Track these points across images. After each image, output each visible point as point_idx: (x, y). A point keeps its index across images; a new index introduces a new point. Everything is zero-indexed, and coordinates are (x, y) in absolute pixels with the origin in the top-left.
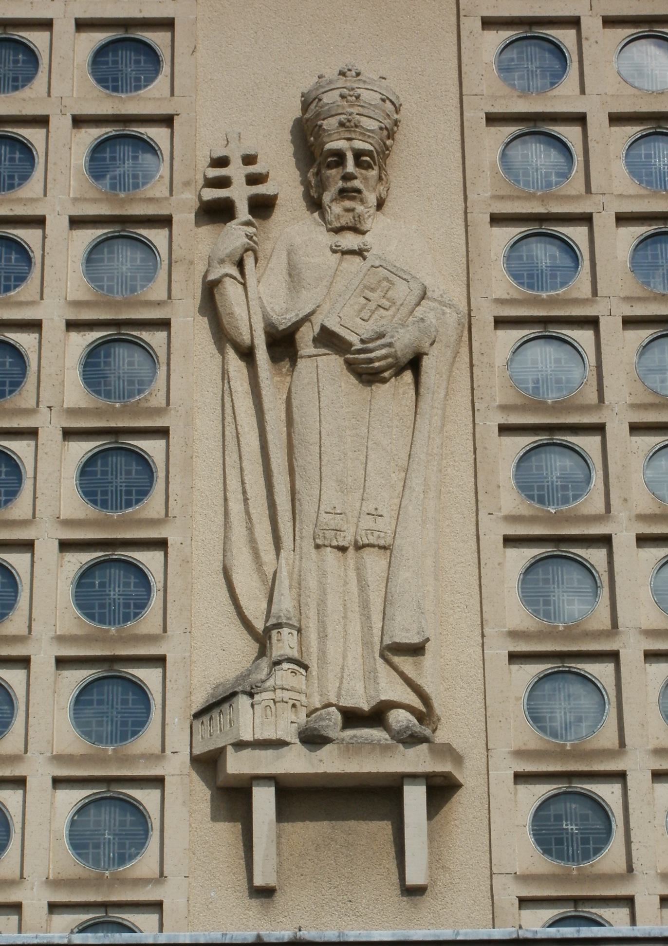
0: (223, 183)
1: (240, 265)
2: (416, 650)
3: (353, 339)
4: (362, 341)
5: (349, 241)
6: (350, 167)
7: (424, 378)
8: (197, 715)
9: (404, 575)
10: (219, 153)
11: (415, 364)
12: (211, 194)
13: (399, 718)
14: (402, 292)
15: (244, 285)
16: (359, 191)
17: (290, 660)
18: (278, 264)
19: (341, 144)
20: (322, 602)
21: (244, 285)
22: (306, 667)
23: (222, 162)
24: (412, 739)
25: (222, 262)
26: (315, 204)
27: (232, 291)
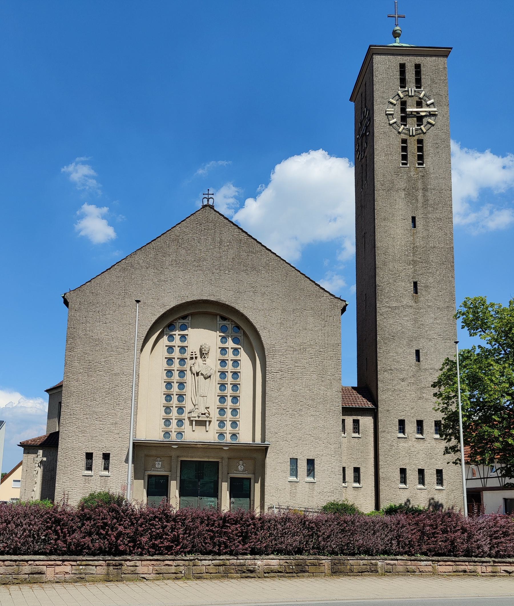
0: (192, 355)
1: (194, 365)
2: (208, 408)
6: (205, 355)
8: (188, 413)
9: (208, 400)
11: (210, 377)
13: (207, 414)
14: (209, 369)
18: (197, 364)
23: (192, 352)
24: (207, 417)
26: (201, 357)
27: (193, 368)
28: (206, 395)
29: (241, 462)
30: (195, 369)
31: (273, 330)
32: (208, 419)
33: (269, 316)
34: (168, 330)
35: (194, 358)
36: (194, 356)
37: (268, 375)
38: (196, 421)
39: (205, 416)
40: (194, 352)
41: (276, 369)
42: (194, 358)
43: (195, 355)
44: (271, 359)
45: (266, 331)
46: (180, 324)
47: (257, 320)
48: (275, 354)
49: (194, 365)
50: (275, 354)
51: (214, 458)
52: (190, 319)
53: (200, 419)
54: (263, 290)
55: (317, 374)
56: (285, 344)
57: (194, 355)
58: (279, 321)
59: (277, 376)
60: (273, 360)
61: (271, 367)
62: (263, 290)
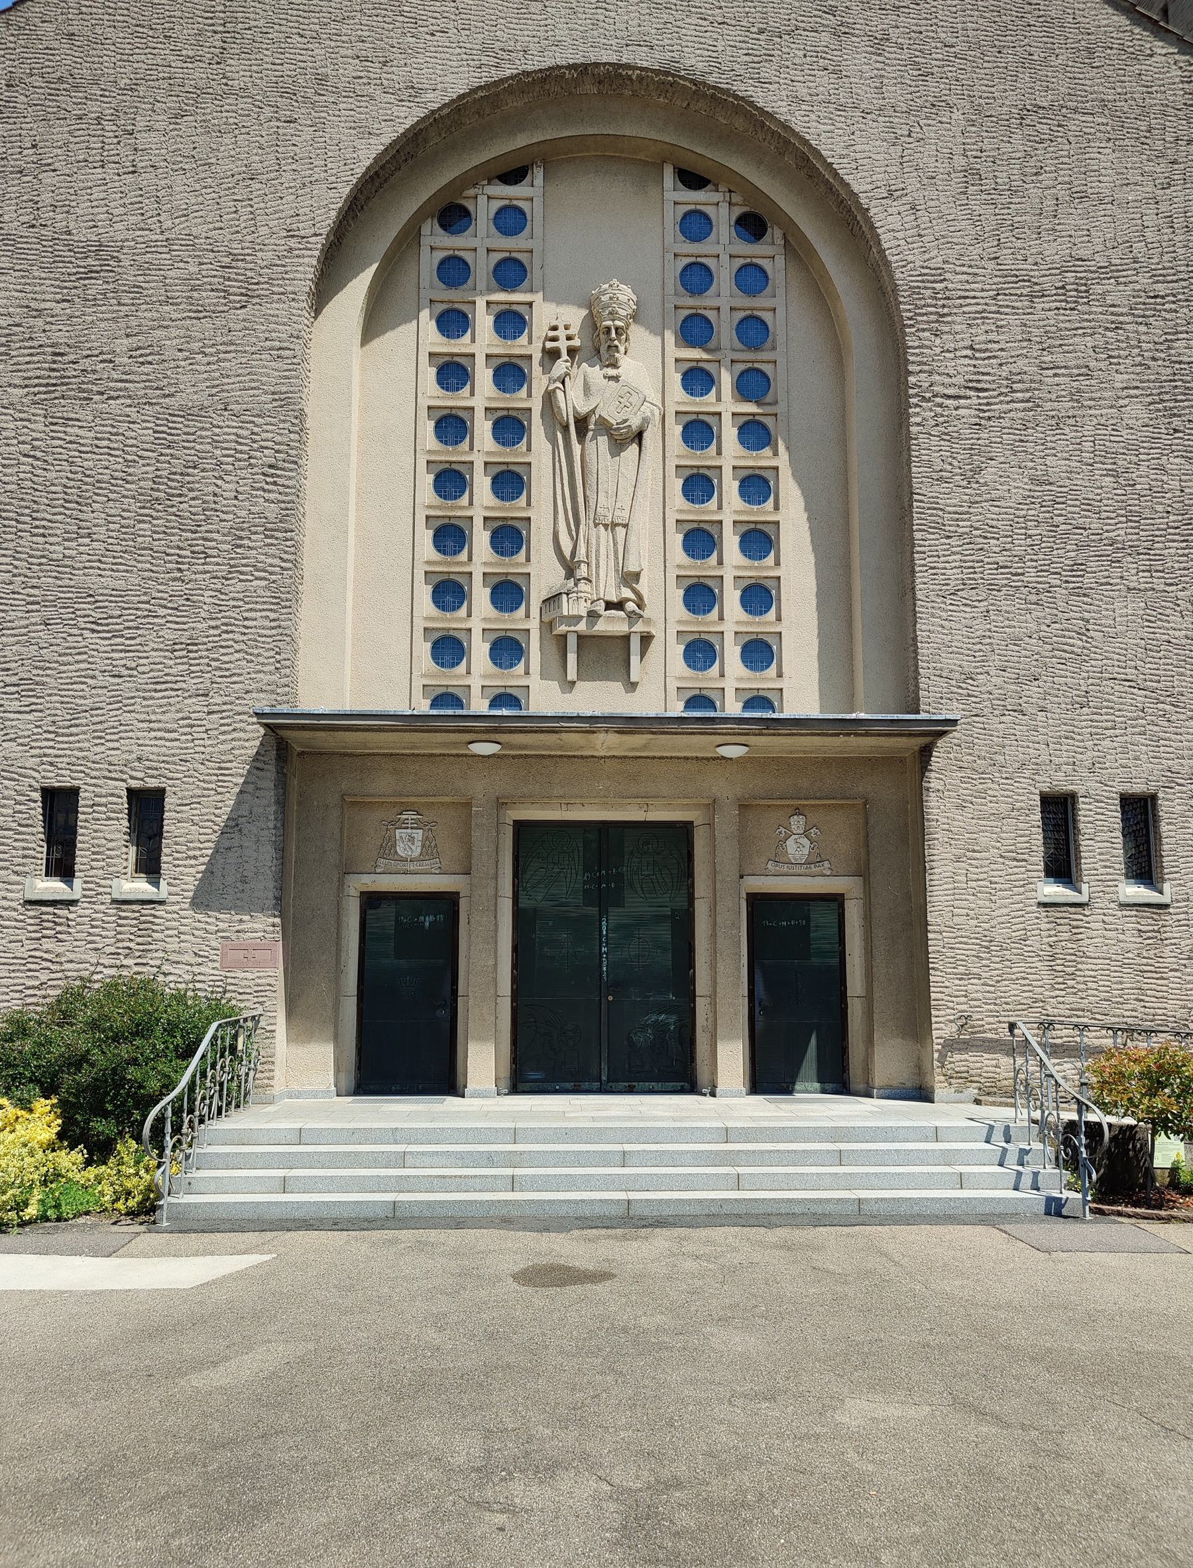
0: (554, 339)
1: (563, 383)
3: (614, 422)
4: (617, 424)
5: (611, 372)
7: (644, 442)
9: (632, 539)
10: (554, 323)
11: (639, 436)
12: (549, 345)
15: (564, 392)
16: (617, 347)
17: (584, 579)
18: (580, 382)
19: (609, 323)
20: (598, 551)
21: (564, 392)
22: (590, 581)
23: (555, 328)
25: (555, 381)
28: (620, 518)
29: (797, 823)
30: (573, 401)
31: (932, 203)
32: (639, 627)
33: (911, 140)
34: (438, 229)
35: (564, 352)
36: (563, 345)
37: (918, 410)
38: (581, 638)
39: (621, 613)
40: (561, 328)
41: (954, 380)
42: (564, 352)
43: (569, 338)
44: (927, 334)
45: (902, 209)
46: (496, 205)
47: (858, 156)
48: (946, 310)
49: (563, 383)
50: (946, 310)
51: (669, 807)
52: (539, 181)
53: (601, 627)
54: (879, 23)
55: (1149, 399)
56: (991, 265)
57: (563, 338)
58: (960, 162)
59: (962, 412)
60: (938, 341)
61: (931, 373)
62: (879, 23)
